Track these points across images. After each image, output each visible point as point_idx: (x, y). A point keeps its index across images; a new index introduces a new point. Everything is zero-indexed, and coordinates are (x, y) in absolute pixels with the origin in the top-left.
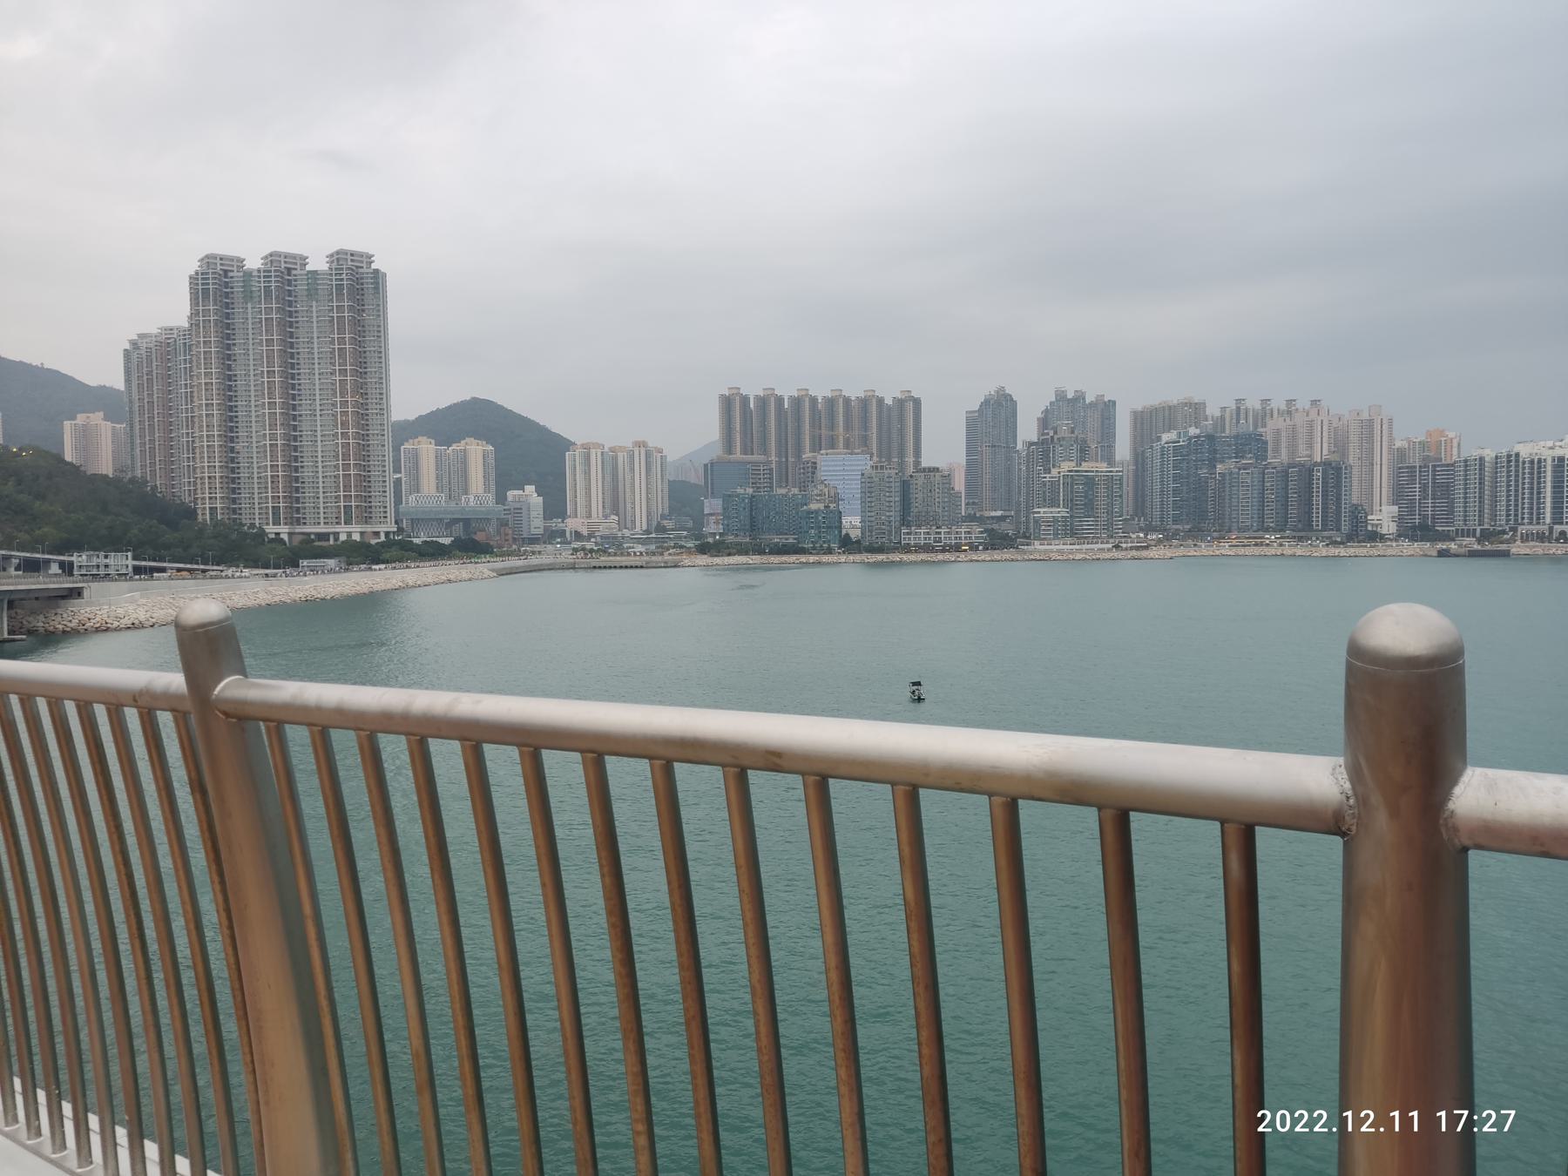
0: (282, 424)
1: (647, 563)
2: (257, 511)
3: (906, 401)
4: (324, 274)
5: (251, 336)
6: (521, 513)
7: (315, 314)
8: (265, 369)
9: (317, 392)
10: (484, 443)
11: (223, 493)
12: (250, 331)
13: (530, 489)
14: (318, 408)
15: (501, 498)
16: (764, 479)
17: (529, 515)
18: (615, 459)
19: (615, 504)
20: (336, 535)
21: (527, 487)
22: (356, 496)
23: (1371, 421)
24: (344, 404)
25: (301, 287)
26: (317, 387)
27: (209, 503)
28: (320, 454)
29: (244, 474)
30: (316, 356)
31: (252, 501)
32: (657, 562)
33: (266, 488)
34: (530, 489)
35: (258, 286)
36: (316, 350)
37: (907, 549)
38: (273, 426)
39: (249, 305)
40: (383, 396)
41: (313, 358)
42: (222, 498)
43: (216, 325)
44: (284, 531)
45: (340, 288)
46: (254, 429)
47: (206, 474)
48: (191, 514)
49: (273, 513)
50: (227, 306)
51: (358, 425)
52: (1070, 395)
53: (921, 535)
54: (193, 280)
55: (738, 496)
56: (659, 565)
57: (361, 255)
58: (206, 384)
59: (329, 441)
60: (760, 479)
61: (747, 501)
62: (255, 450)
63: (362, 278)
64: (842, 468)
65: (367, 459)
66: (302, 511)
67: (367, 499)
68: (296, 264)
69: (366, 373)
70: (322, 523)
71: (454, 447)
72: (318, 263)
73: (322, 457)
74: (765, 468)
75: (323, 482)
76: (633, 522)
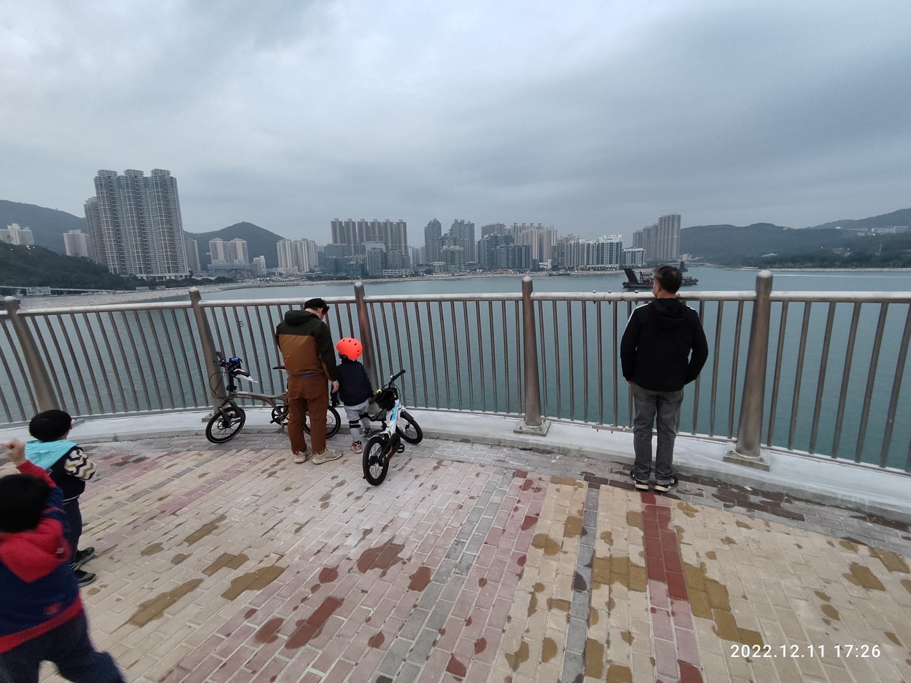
13: (262, 257)
15: (251, 260)
18: (296, 245)
19: (297, 262)
20: (165, 277)
21: (261, 256)
23: (550, 231)
25: (142, 183)
27: (113, 265)
34: (262, 257)
35: (123, 182)
37: (384, 277)
38: (135, 237)
40: (179, 224)
43: (107, 198)
44: (144, 276)
45: (156, 184)
48: (107, 270)
51: (169, 236)
52: (459, 222)
53: (389, 272)
54: (96, 179)
57: (165, 171)
67: (176, 263)
71: (231, 242)
72: (148, 174)
76: (304, 269)
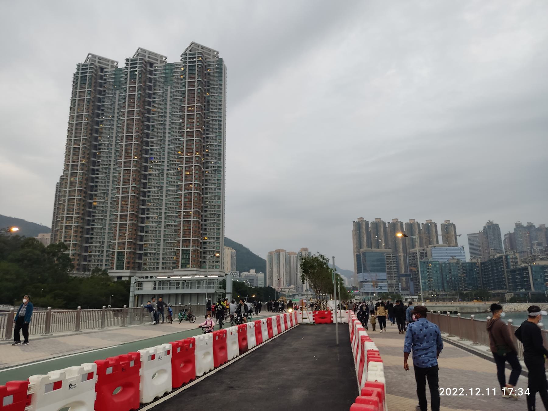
0: (134, 180)
1: (462, 308)
2: (104, 258)
3: (449, 225)
4: (179, 65)
5: (116, 115)
6: (253, 282)
7: (169, 95)
8: (125, 135)
9: (166, 155)
10: (231, 248)
11: (76, 241)
12: (116, 111)
13: (252, 271)
14: (166, 168)
16: (393, 262)
17: (257, 283)
21: (250, 270)
22: (194, 241)
24: (189, 160)
25: (160, 76)
26: (166, 151)
28: (164, 207)
29: (97, 226)
30: (167, 127)
31: (101, 249)
32: (471, 308)
33: (115, 236)
36: (168, 123)
39: (118, 92)
41: (165, 129)
42: (75, 245)
43: (88, 102)
45: (192, 68)
46: (110, 188)
47: (64, 225)
49: (118, 258)
50: (100, 93)
51: (199, 179)
55: (428, 262)
56: (474, 311)
58: (74, 149)
59: (173, 195)
60: (391, 262)
61: (438, 266)
62: (109, 205)
63: (209, 66)
64: (446, 255)
65: (204, 209)
66: (144, 257)
68: (157, 60)
69: (208, 138)
70: (160, 268)
73: (166, 209)
74: (394, 255)
75: (165, 231)
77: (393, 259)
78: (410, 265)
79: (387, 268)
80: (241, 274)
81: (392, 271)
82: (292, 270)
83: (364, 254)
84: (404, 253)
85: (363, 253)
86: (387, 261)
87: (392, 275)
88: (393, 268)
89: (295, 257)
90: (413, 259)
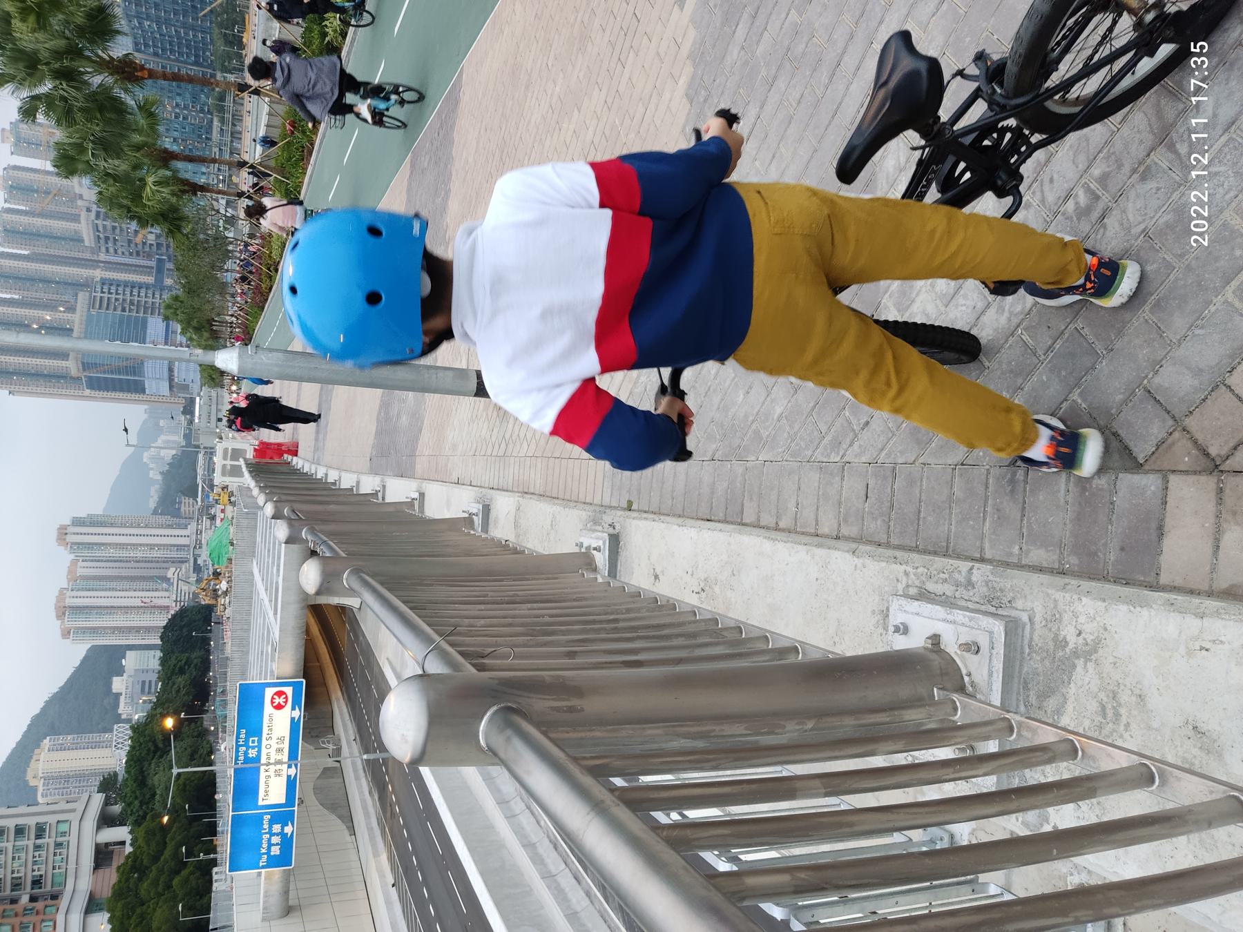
6: (150, 682)
13: (118, 684)
21: (114, 691)
60: (117, 300)
74: (99, 290)
76: (180, 547)
77: (110, 293)
78: (131, 254)
79: (134, 314)
80: (124, 717)
81: (145, 302)
82: (124, 573)
83: (86, 366)
84: (95, 268)
85: (84, 370)
86: (115, 309)
87: (157, 305)
88: (136, 298)
89: (85, 564)
90: (115, 244)
